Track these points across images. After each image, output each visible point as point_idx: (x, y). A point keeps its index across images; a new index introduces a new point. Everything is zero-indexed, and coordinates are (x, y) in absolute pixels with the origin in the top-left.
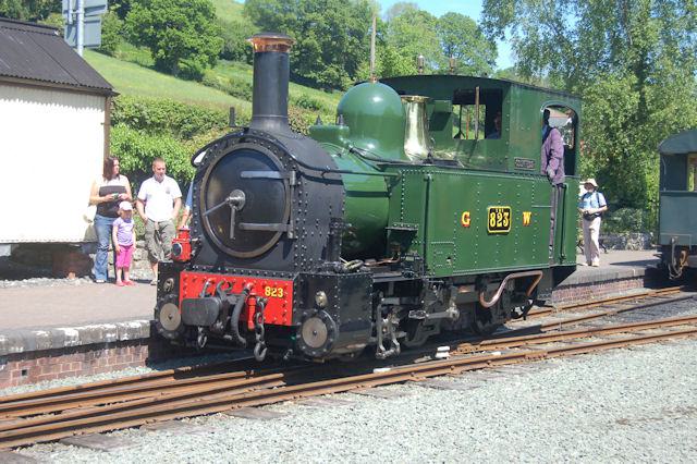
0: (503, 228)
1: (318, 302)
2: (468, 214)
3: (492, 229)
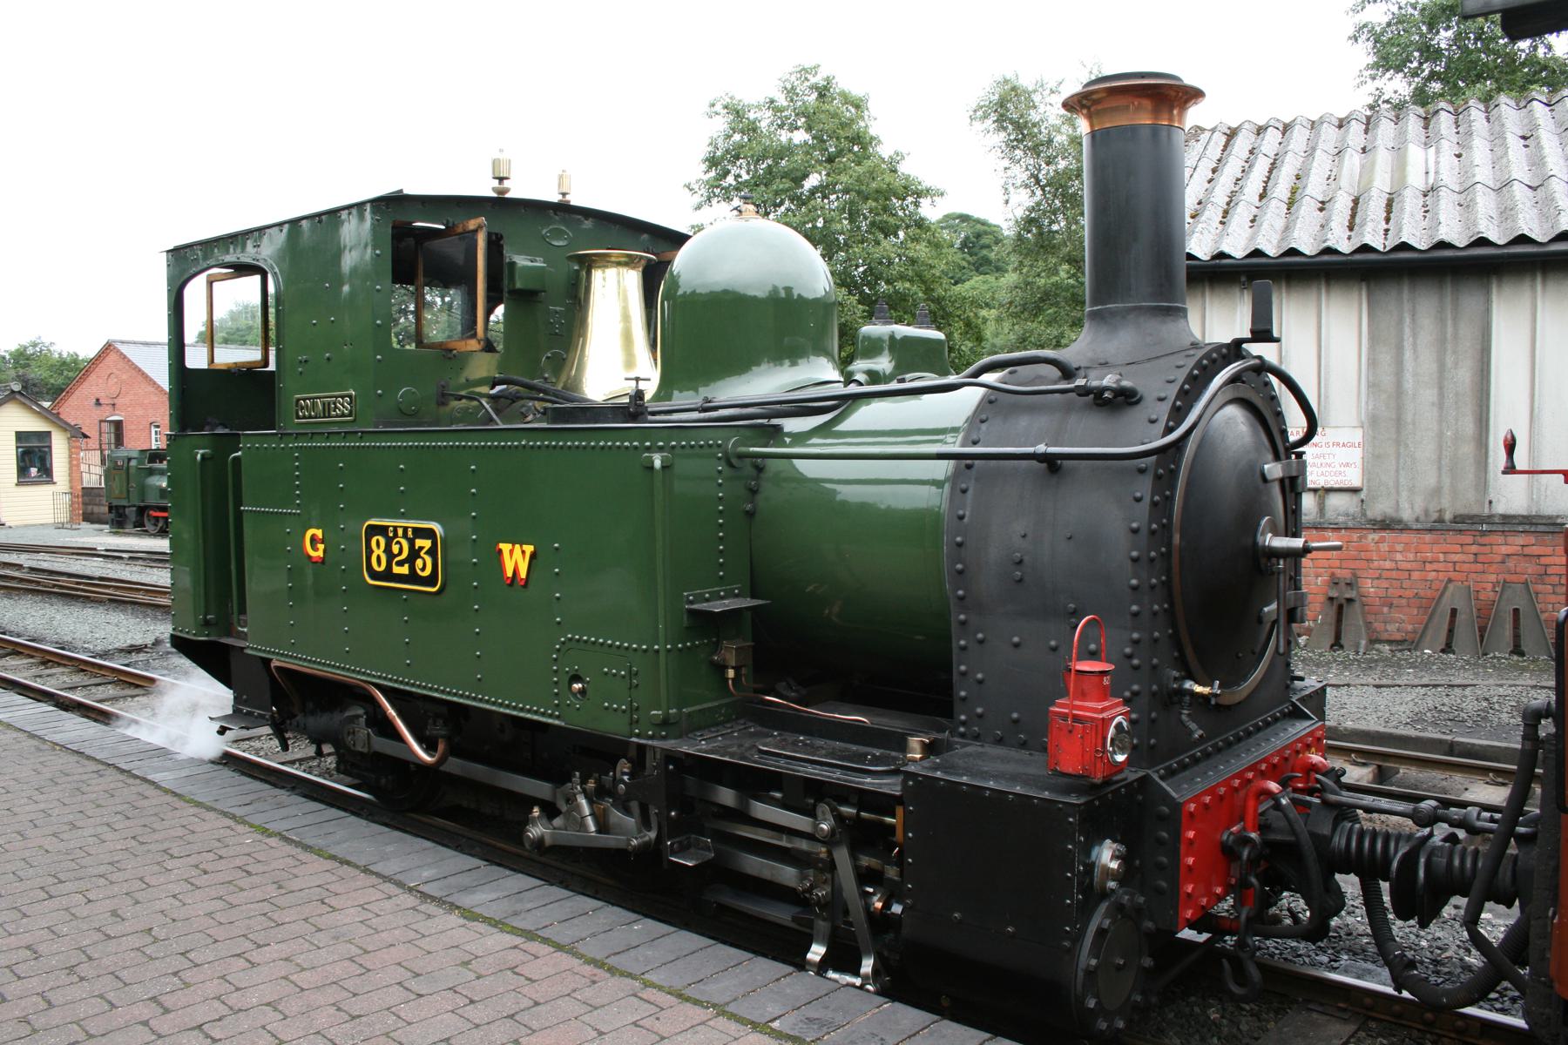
2: (319, 533)
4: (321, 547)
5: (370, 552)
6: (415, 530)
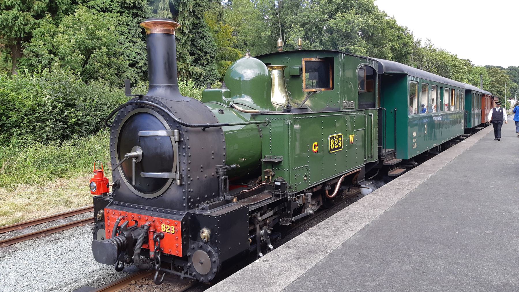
0: (339, 148)
1: (202, 237)
2: (316, 143)
3: (332, 150)
4: (317, 147)
5: (331, 144)
6: (339, 136)
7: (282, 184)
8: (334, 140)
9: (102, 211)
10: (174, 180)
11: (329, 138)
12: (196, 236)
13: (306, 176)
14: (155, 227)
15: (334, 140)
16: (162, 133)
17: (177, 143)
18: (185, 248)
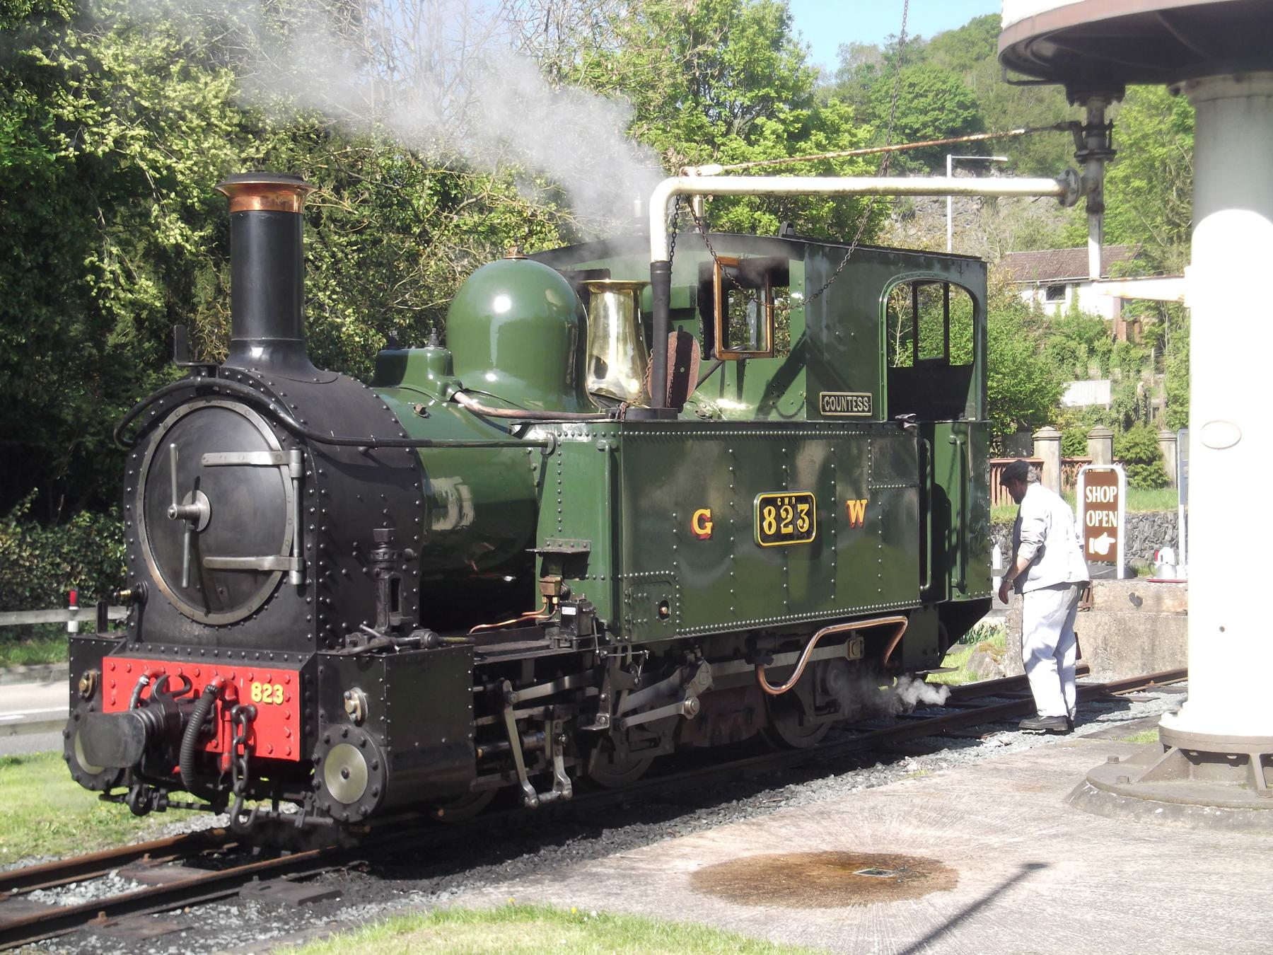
2: (707, 513)
3: (766, 538)
4: (709, 525)
5: (762, 519)
7: (580, 611)
8: (778, 509)
9: (92, 673)
10: (286, 574)
11: (757, 502)
12: (337, 712)
13: (665, 604)
14: (236, 691)
15: (778, 509)
16: (264, 458)
17: (295, 482)
18: (308, 737)
